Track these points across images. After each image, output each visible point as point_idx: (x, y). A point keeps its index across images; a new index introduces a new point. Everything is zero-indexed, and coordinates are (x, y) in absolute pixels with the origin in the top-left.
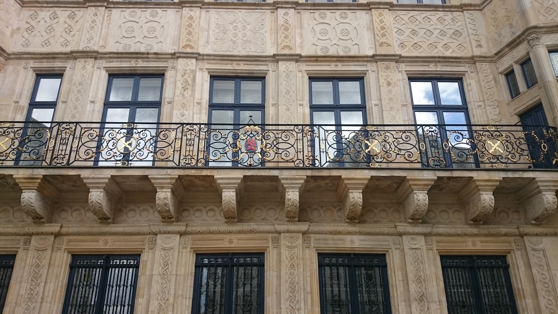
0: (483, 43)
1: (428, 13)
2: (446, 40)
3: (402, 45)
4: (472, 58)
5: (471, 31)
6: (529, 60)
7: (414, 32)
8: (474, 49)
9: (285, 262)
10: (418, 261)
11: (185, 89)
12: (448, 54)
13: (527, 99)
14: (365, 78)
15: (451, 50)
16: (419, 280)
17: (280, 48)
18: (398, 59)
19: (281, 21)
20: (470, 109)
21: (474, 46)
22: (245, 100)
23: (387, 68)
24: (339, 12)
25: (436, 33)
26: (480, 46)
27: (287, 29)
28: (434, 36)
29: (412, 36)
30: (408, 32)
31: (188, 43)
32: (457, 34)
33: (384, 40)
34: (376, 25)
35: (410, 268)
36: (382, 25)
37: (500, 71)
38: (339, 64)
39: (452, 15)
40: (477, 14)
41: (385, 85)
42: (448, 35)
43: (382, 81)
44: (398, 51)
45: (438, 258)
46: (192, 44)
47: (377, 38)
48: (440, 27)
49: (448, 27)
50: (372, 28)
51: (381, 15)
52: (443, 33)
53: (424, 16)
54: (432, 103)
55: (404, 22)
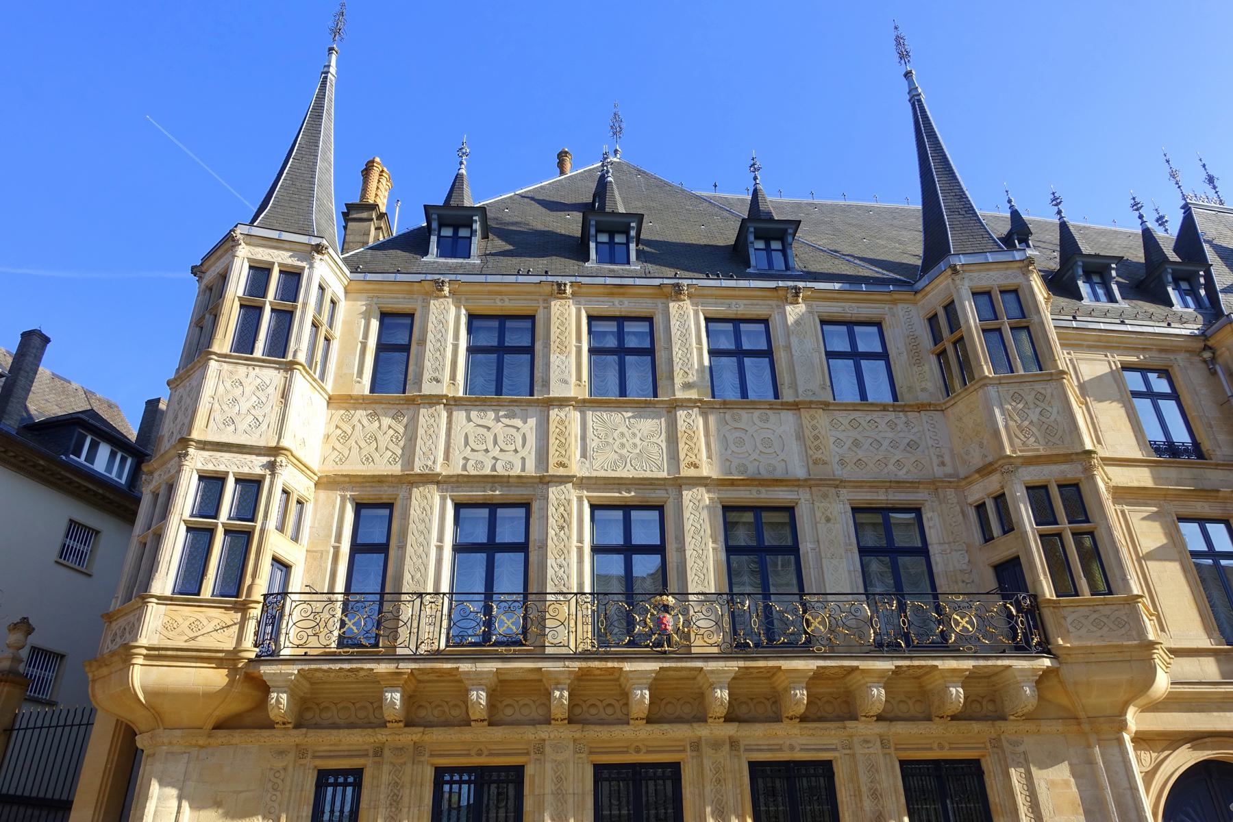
0: (947, 459)
1: (875, 415)
2: (898, 455)
3: (842, 462)
4: (933, 482)
5: (930, 442)
6: (1004, 494)
7: (856, 443)
9: (709, 774)
10: (873, 769)
11: (562, 528)
12: (902, 475)
13: (1003, 549)
15: (905, 470)
16: (875, 795)
18: (839, 484)
20: (931, 553)
21: (935, 465)
22: (638, 539)
23: (825, 496)
24: (757, 413)
25: (886, 443)
26: (943, 464)
28: (883, 448)
30: (849, 443)
31: (561, 459)
32: (912, 445)
33: (818, 455)
34: (807, 432)
35: (864, 779)
37: (970, 501)
38: (763, 489)
40: (937, 416)
41: (823, 521)
42: (902, 447)
43: (818, 514)
44: (840, 473)
45: (897, 765)
46: (565, 461)
47: (810, 452)
48: (890, 435)
49: (902, 435)
50: (800, 437)
51: (813, 418)
52: (894, 444)
53: (868, 418)
54: (884, 543)
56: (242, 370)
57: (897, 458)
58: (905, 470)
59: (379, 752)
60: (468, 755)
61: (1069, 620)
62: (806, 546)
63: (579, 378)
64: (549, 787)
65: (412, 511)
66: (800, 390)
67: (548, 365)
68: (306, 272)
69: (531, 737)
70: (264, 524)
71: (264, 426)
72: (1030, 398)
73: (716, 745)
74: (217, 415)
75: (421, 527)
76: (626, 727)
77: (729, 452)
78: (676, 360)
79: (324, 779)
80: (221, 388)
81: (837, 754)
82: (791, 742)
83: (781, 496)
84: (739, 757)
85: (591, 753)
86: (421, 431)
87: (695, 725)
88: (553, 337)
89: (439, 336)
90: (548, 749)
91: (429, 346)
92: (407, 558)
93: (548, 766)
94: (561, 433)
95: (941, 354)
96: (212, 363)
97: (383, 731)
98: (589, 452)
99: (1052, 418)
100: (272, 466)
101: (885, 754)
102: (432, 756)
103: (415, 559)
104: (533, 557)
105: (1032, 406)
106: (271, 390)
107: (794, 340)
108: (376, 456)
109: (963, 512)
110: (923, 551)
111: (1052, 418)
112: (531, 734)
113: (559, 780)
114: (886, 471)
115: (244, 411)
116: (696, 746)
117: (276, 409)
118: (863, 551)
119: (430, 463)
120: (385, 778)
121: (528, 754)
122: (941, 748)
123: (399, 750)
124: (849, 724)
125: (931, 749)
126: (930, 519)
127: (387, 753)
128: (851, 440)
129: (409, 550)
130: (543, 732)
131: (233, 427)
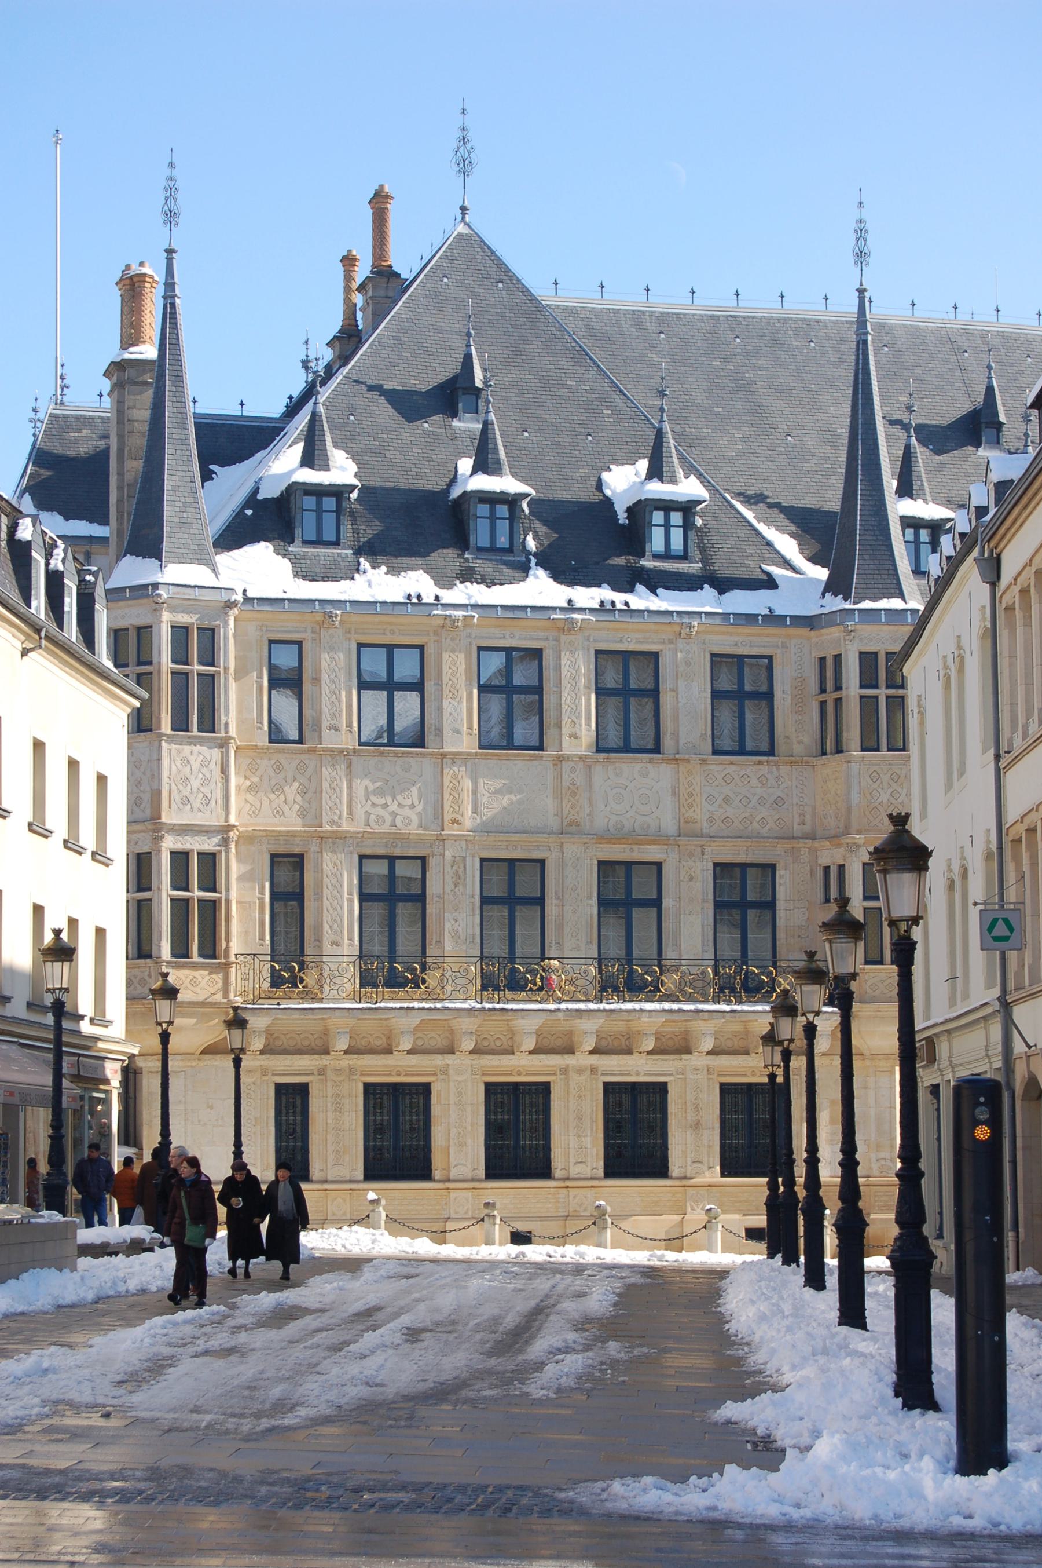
0: (808, 818)
3: (711, 820)
7: (727, 800)
8: (796, 827)
14: (664, 865)
16: (697, 1108)
17: (565, 823)
19: (566, 783)
25: (754, 800)
27: (574, 794)
28: (751, 805)
29: (724, 805)
30: (720, 801)
31: (455, 816)
32: (779, 802)
33: (690, 814)
36: (690, 789)
39: (778, 769)
41: (687, 879)
43: (683, 873)
46: (459, 818)
47: (683, 810)
48: (759, 791)
52: (762, 801)
55: (716, 783)
56: (187, 749)
57: (762, 815)
58: (767, 828)
59: (322, 1071)
60: (390, 1075)
61: (869, 983)
62: (667, 902)
63: (470, 728)
64: (453, 1099)
65: (325, 866)
66: (682, 741)
67: (440, 709)
68: (222, 630)
69: (439, 1063)
70: (227, 895)
71: (213, 802)
72: (885, 778)
73: (580, 1071)
74: (175, 795)
75: (334, 881)
76: (511, 1056)
77: (608, 808)
78: (564, 707)
79: (281, 1090)
80: (173, 767)
81: (672, 1078)
82: (637, 1068)
83: (652, 853)
84: (597, 1080)
85: (483, 1075)
86: (325, 785)
87: (566, 1056)
88: (445, 679)
89: (333, 677)
90: (451, 1072)
91: (325, 689)
92: (325, 911)
93: (452, 1084)
94: (455, 789)
95: (823, 704)
96: (164, 744)
97: (327, 1057)
98: (481, 808)
99: (900, 800)
100: (225, 842)
101: (709, 1079)
102: (362, 1075)
103: (331, 911)
104: (430, 909)
105: (885, 785)
106: (212, 766)
107: (682, 685)
108: (286, 808)
109: (812, 871)
110: (771, 905)
111: (900, 800)
112: (439, 1060)
113: (460, 1093)
114: (750, 828)
115: (195, 790)
116: (565, 1070)
117: (219, 785)
118: (718, 905)
119: (336, 818)
120: (330, 1091)
121: (435, 1075)
122: (753, 1075)
123: (338, 1071)
124: (684, 1056)
125: (745, 1075)
126: (781, 877)
127: (329, 1074)
128: (722, 797)
129: (326, 903)
130: (449, 1059)
131: (189, 806)
